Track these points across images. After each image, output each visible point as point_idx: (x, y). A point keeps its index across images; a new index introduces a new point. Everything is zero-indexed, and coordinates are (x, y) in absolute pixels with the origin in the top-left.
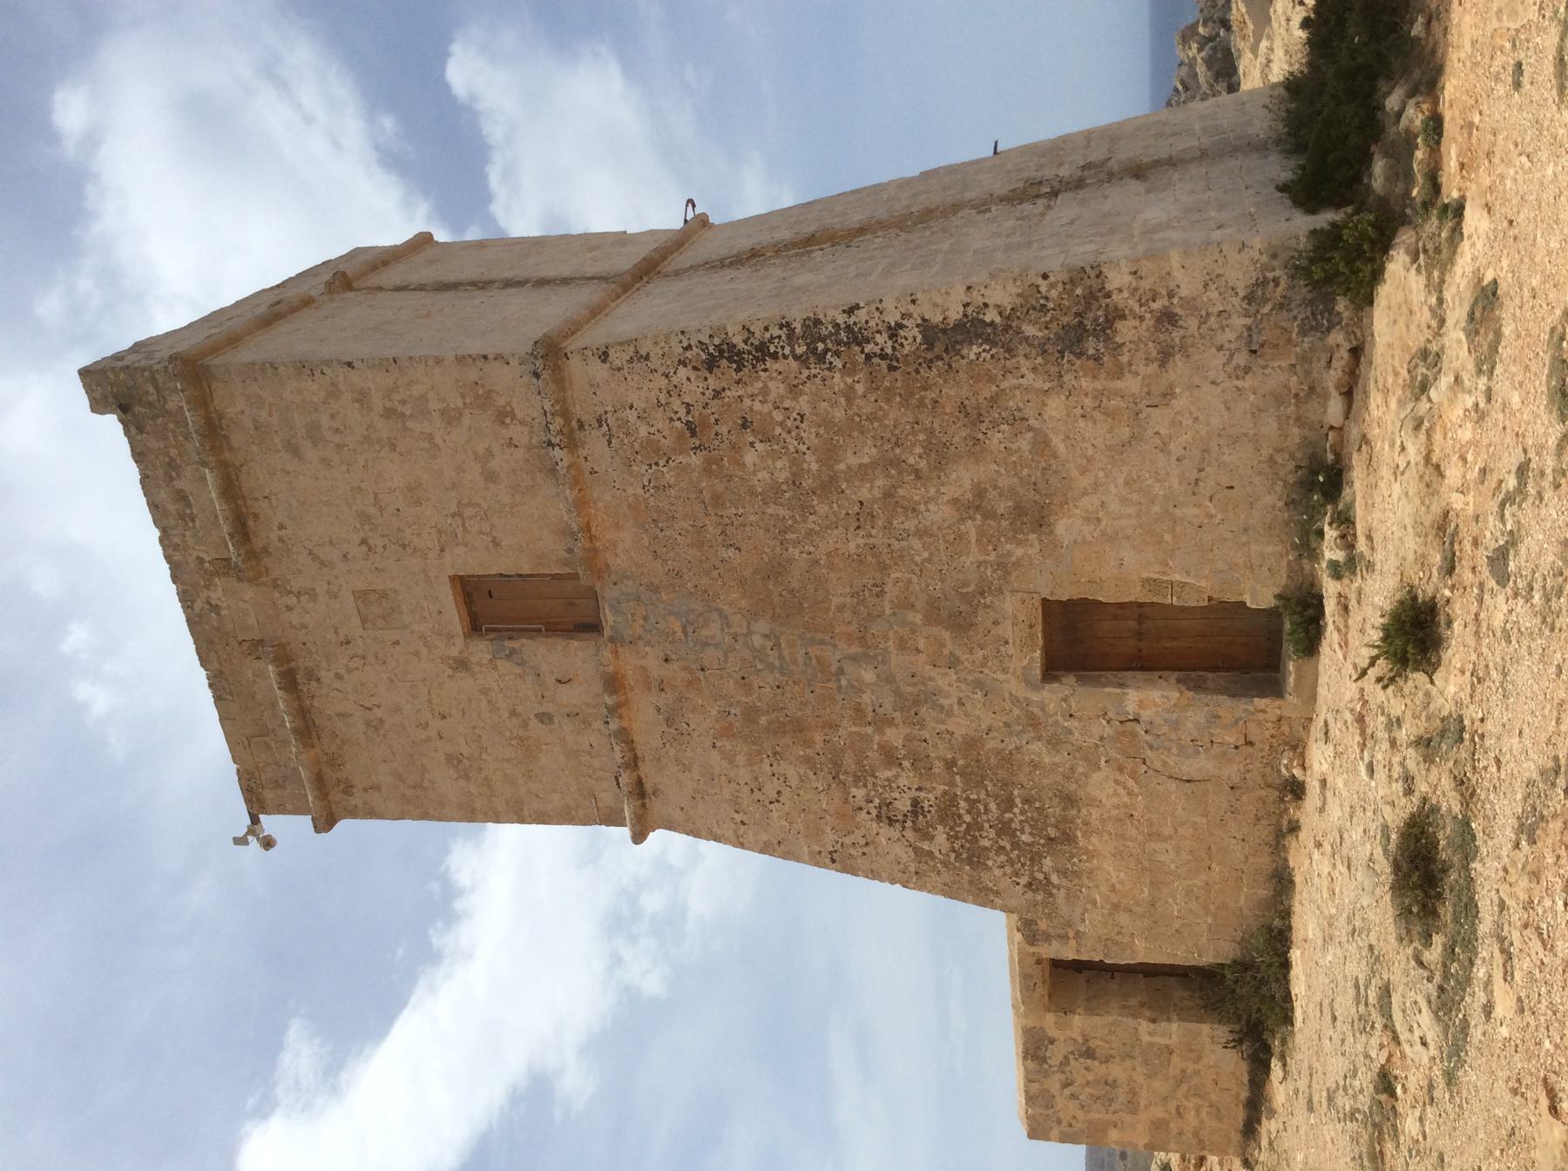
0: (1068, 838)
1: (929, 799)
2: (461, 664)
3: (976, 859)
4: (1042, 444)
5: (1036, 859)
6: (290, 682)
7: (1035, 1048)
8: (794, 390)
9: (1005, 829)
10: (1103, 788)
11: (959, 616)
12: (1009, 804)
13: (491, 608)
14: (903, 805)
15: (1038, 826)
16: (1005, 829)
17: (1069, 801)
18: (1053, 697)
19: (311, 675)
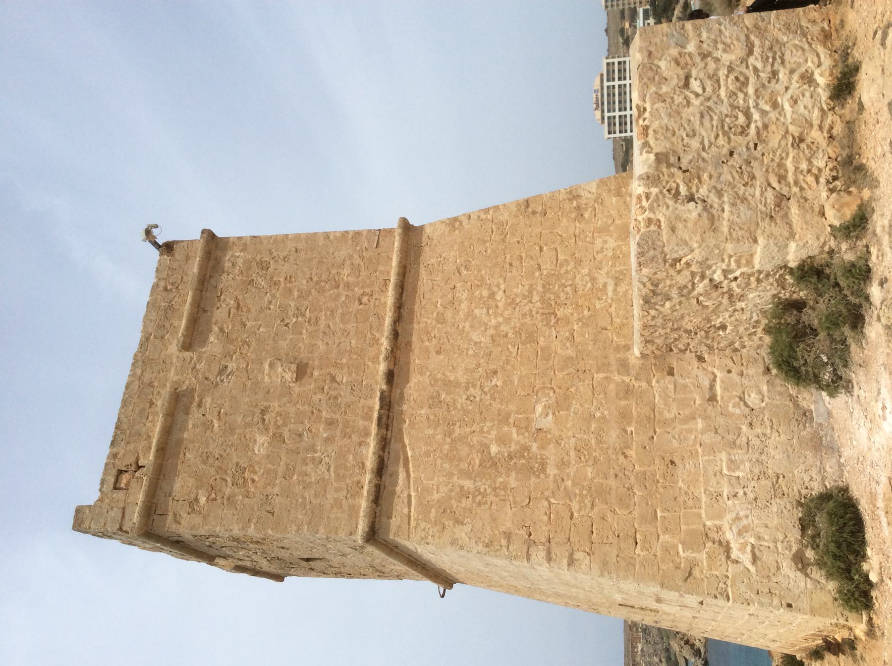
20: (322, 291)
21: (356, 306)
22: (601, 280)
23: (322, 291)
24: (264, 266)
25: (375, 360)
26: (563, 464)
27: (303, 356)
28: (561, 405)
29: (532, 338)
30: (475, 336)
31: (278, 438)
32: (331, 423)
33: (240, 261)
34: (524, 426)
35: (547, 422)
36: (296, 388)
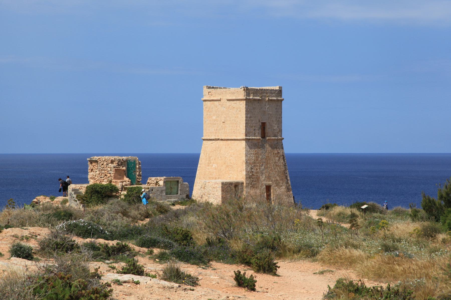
0: (253, 188)
1: (254, 173)
2: (259, 121)
3: (250, 178)
4: (281, 186)
5: (251, 184)
6: (259, 100)
7: (231, 184)
8: (282, 163)
9: (253, 181)
10: (258, 191)
11: (269, 178)
12: (255, 181)
13: (263, 126)
14: (253, 170)
15: (254, 185)
16: (253, 181)
17: (257, 188)
18: (265, 187)
19: (258, 103)
20: (236, 124)
21: (233, 131)
22: (231, 175)
23: (236, 124)
24: (240, 111)
25: (225, 136)
26: (208, 169)
27: (226, 122)
28: (215, 169)
29: (225, 163)
30: (226, 154)
31: (215, 120)
32: (217, 130)
33: (241, 106)
34: (213, 163)
35: (214, 167)
36: (221, 122)
